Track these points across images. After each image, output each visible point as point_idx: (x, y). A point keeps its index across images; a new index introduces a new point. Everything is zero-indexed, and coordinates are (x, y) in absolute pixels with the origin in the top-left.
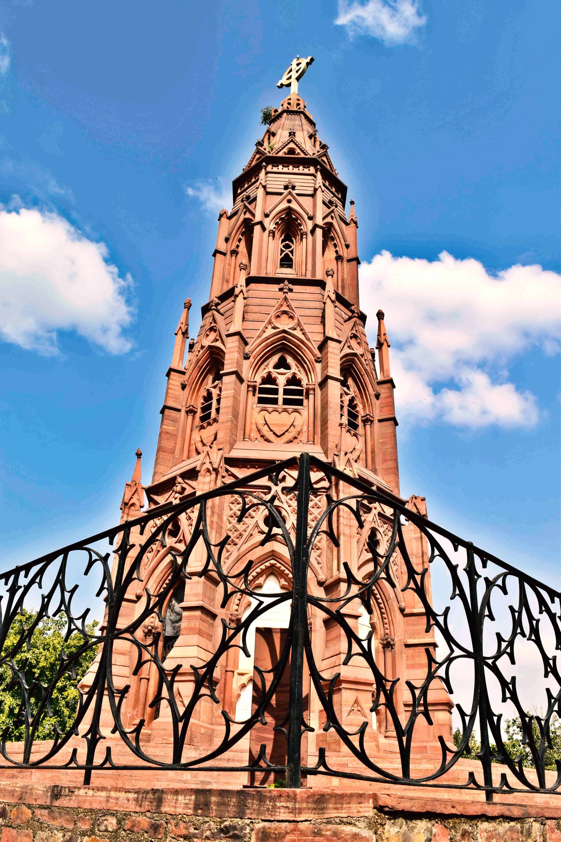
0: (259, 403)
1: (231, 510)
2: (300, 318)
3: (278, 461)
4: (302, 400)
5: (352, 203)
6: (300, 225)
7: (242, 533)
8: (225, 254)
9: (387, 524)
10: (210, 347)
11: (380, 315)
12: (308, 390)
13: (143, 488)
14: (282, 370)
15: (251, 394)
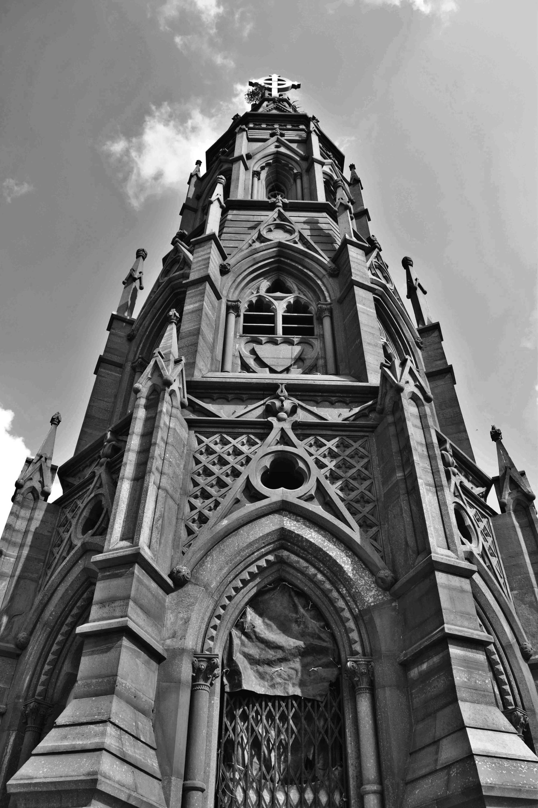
0: (244, 332)
1: (197, 464)
2: (302, 231)
3: (282, 384)
4: (313, 329)
5: (352, 167)
6: (292, 169)
7: (220, 500)
8: (195, 211)
9: (474, 507)
10: (170, 281)
11: (406, 263)
12: (320, 311)
13: (53, 469)
14: (278, 294)
15: (232, 317)
